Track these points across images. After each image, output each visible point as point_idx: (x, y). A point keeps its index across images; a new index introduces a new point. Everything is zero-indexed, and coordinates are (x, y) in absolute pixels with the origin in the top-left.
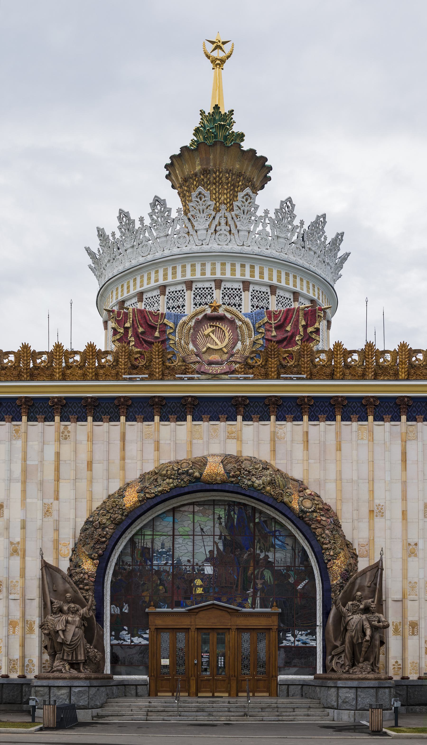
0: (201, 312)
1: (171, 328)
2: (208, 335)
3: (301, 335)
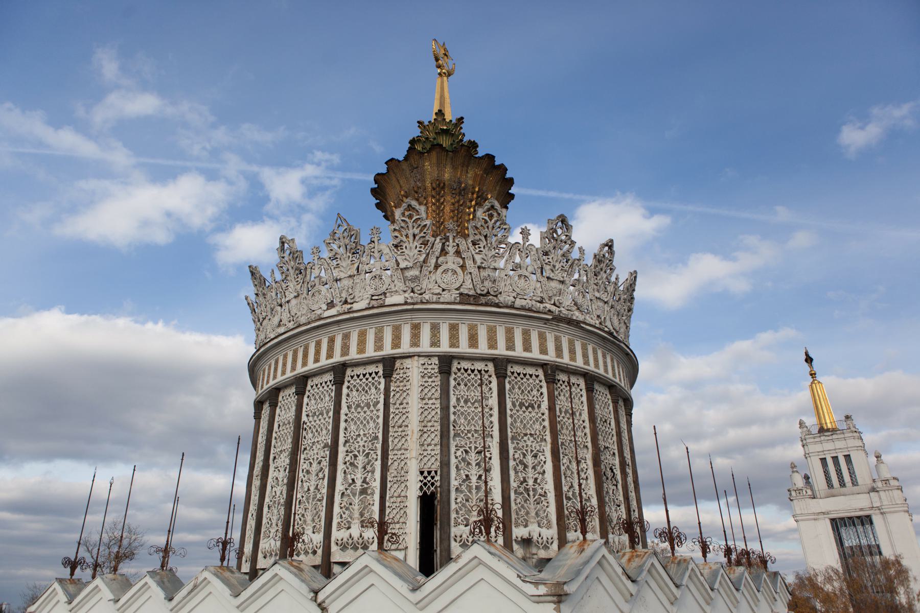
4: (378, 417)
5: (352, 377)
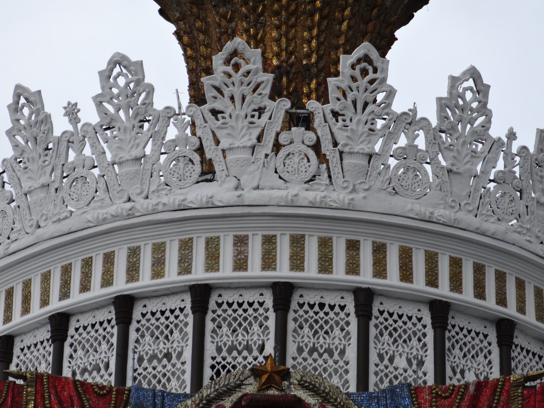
0: (229, 391)
4: (184, 372)
5: (144, 315)
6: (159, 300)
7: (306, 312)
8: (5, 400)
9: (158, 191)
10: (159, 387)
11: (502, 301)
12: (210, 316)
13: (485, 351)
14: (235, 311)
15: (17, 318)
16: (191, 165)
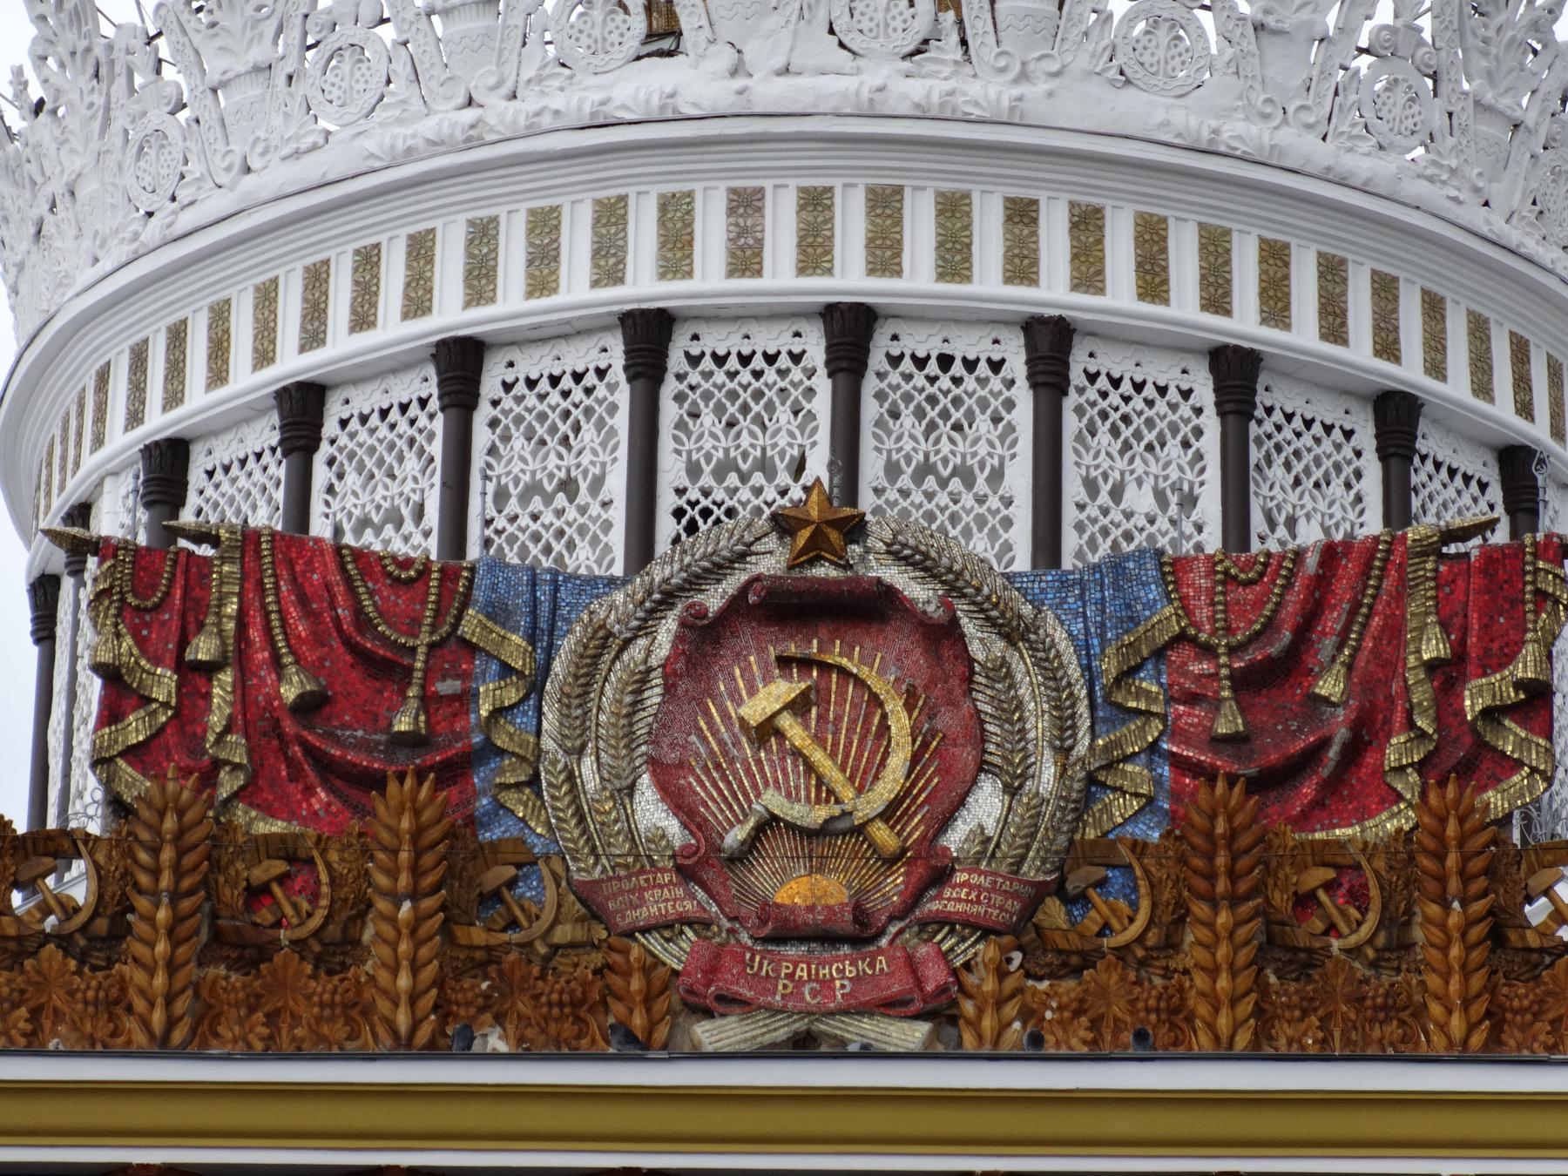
0: (717, 570)
1: (506, 670)
2: (767, 731)
3: (1423, 735)
4: (607, 526)
5: (508, 387)
6: (545, 349)
7: (908, 377)
8: (167, 594)
9: (540, 79)
10: (547, 563)
11: (1388, 348)
12: (670, 387)
13: (1348, 471)
14: (732, 375)
15: (198, 397)
16: (621, 16)
